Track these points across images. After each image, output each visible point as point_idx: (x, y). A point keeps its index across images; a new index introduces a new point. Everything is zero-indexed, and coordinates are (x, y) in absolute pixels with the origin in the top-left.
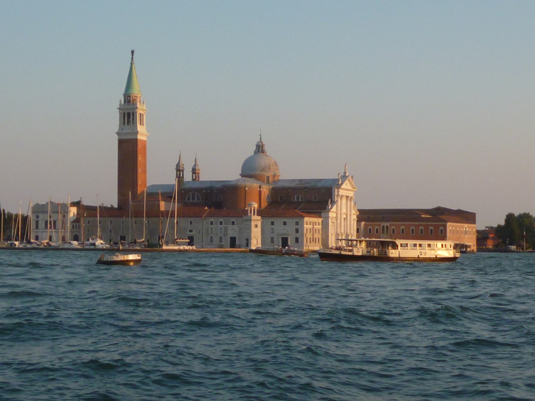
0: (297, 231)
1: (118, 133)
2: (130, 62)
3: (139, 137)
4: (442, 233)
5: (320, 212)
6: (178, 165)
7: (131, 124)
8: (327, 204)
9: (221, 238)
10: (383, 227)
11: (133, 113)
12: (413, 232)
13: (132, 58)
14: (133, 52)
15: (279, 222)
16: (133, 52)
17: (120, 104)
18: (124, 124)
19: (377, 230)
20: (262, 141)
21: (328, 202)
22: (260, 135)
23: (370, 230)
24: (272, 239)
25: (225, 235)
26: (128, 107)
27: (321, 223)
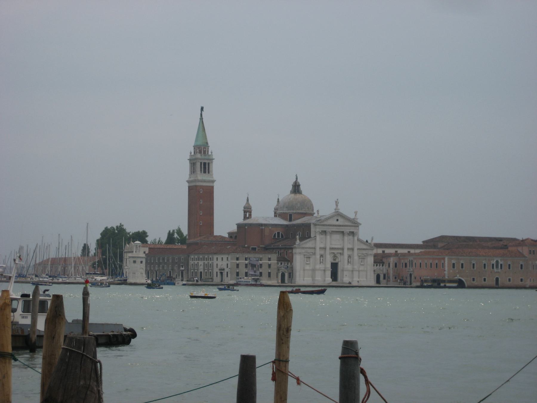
1: (188, 182)
5: (292, 249)
6: (244, 208)
7: (195, 173)
8: (296, 240)
10: (410, 260)
13: (201, 115)
14: (202, 109)
15: (220, 257)
16: (202, 109)
17: (191, 155)
18: (192, 173)
20: (298, 180)
22: (296, 176)
25: (198, 270)
26: (194, 157)
27: (276, 258)
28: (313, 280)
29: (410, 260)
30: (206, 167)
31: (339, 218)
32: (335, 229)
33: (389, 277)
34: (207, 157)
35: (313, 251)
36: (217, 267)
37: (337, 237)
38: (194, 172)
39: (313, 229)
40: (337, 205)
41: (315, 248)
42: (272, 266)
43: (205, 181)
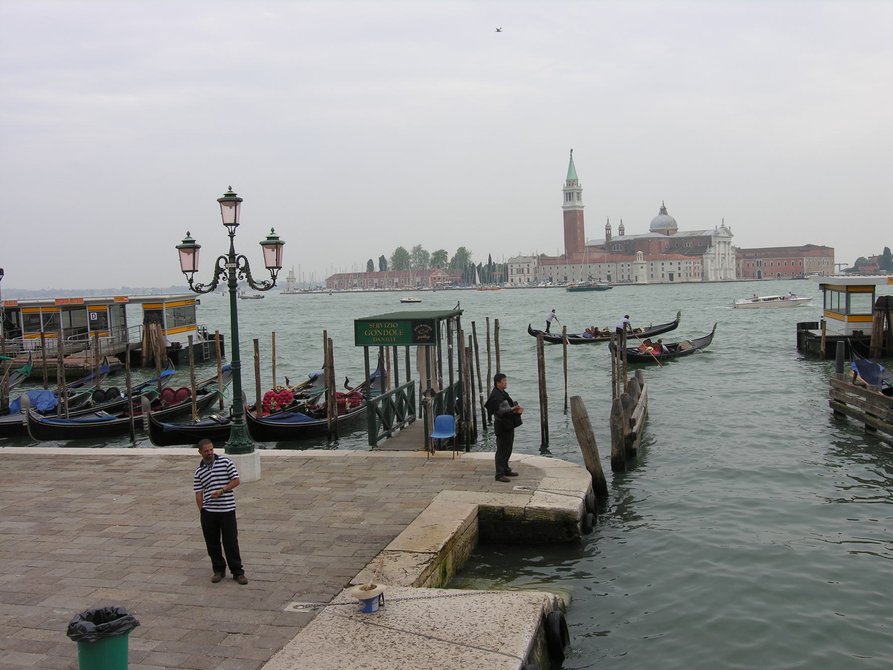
0: (679, 268)
1: (563, 207)
2: (570, 157)
3: (577, 209)
4: (800, 265)
9: (629, 275)
10: (758, 261)
11: (572, 193)
12: (779, 265)
13: (571, 155)
15: (667, 263)
17: (564, 187)
18: (567, 200)
19: (753, 264)
21: (707, 246)
23: (748, 264)
24: (663, 274)
25: (632, 273)
26: (569, 189)
28: (716, 277)
29: (758, 261)
30: (579, 194)
31: (724, 231)
32: (723, 240)
33: (739, 274)
34: (579, 188)
35: (713, 256)
36: (663, 270)
37: (722, 245)
38: (570, 200)
39: (713, 240)
40: (723, 222)
41: (715, 254)
42: (699, 268)
43: (579, 207)
